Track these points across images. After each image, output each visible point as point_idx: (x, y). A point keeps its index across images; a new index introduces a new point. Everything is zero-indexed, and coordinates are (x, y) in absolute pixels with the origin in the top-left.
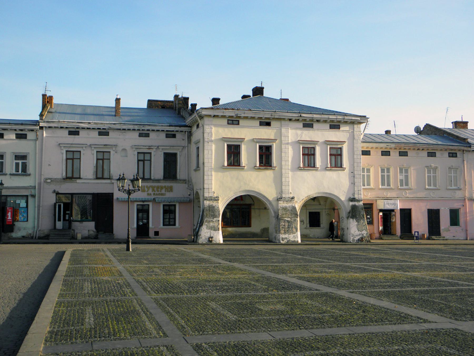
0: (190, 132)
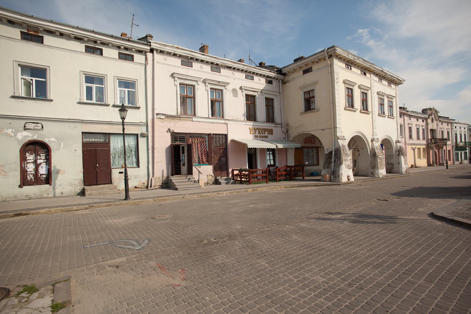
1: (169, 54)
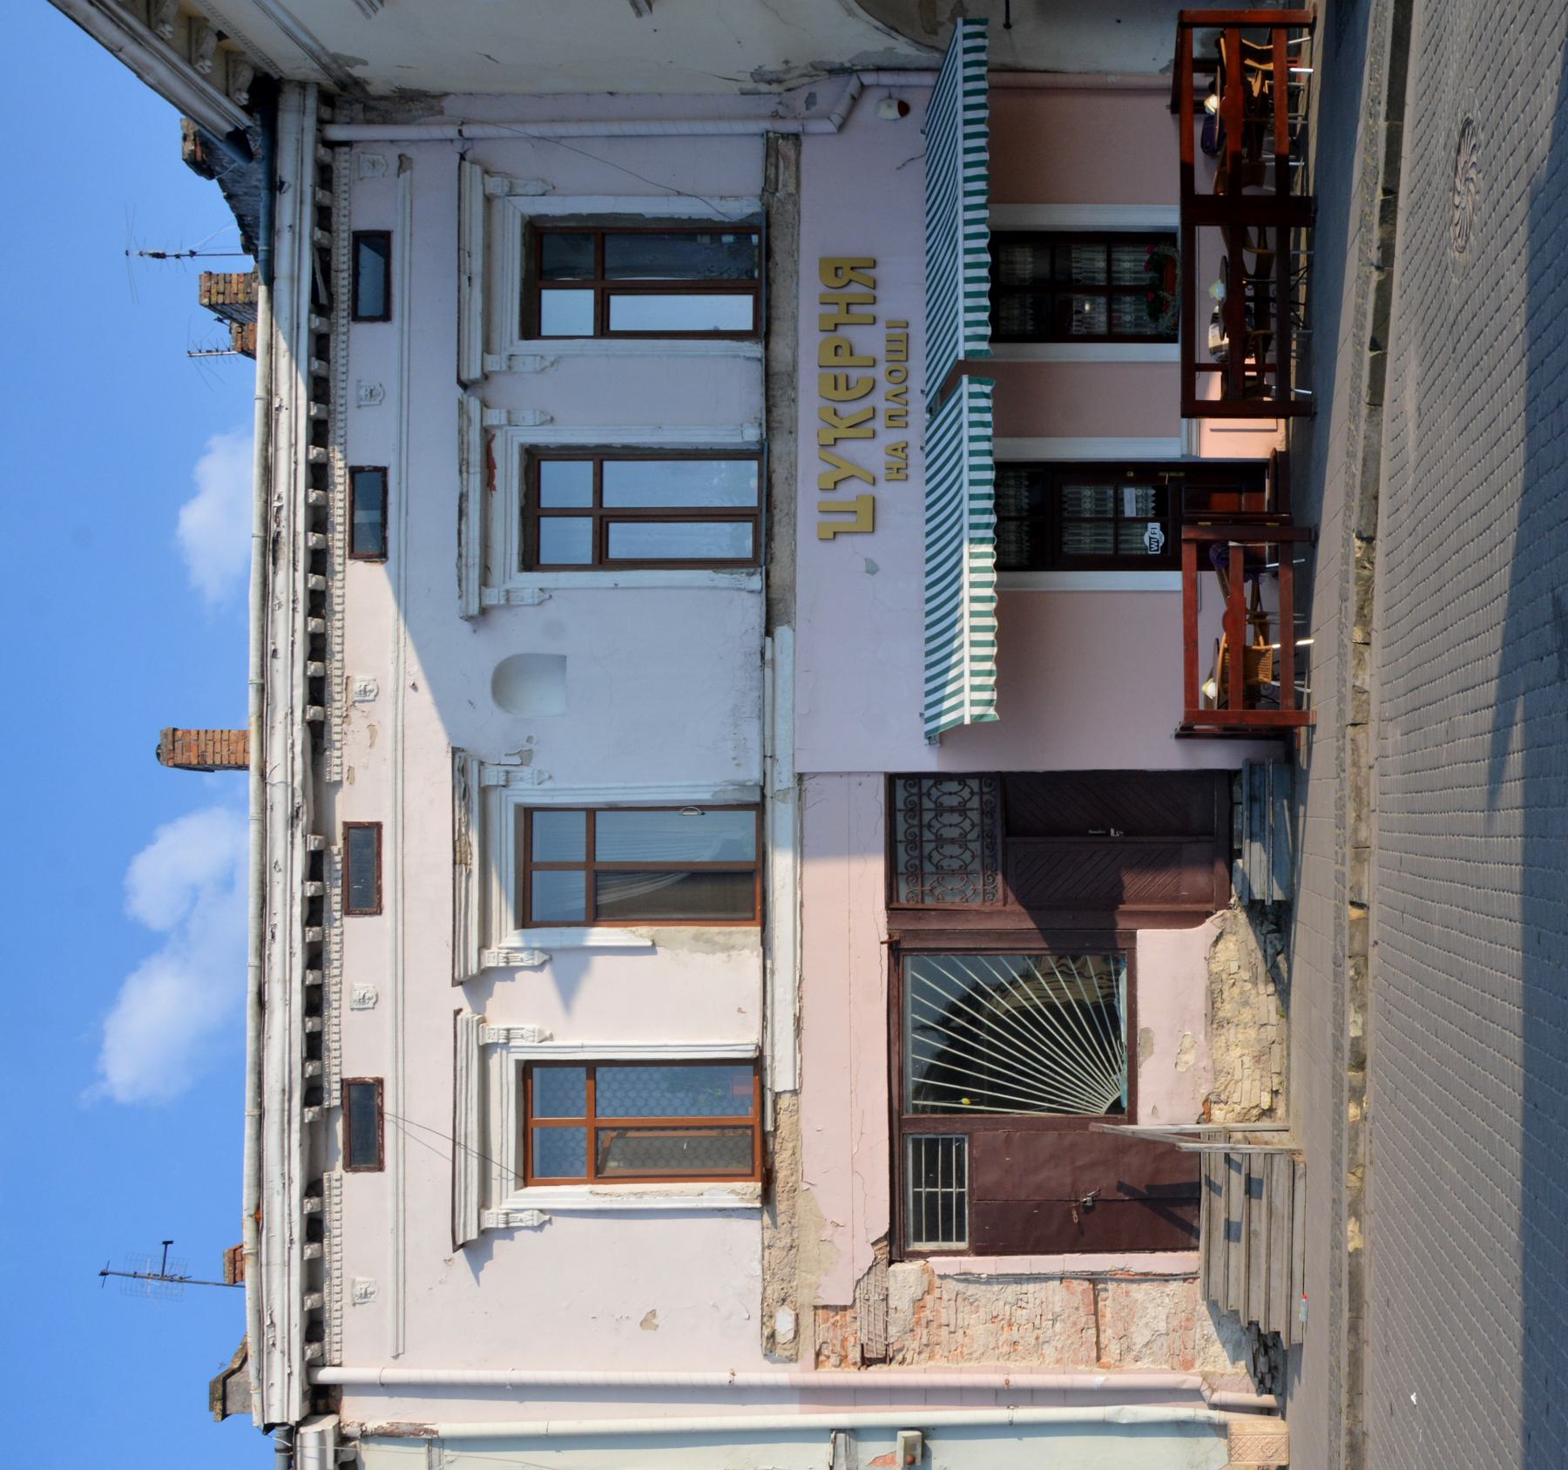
0: (326, 99)
1: (314, 1277)
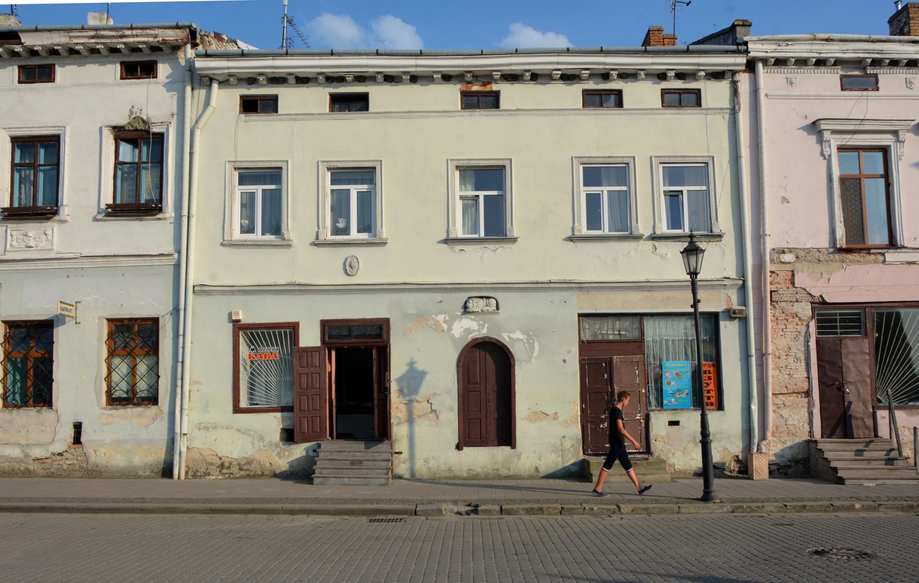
1: (802, 62)
